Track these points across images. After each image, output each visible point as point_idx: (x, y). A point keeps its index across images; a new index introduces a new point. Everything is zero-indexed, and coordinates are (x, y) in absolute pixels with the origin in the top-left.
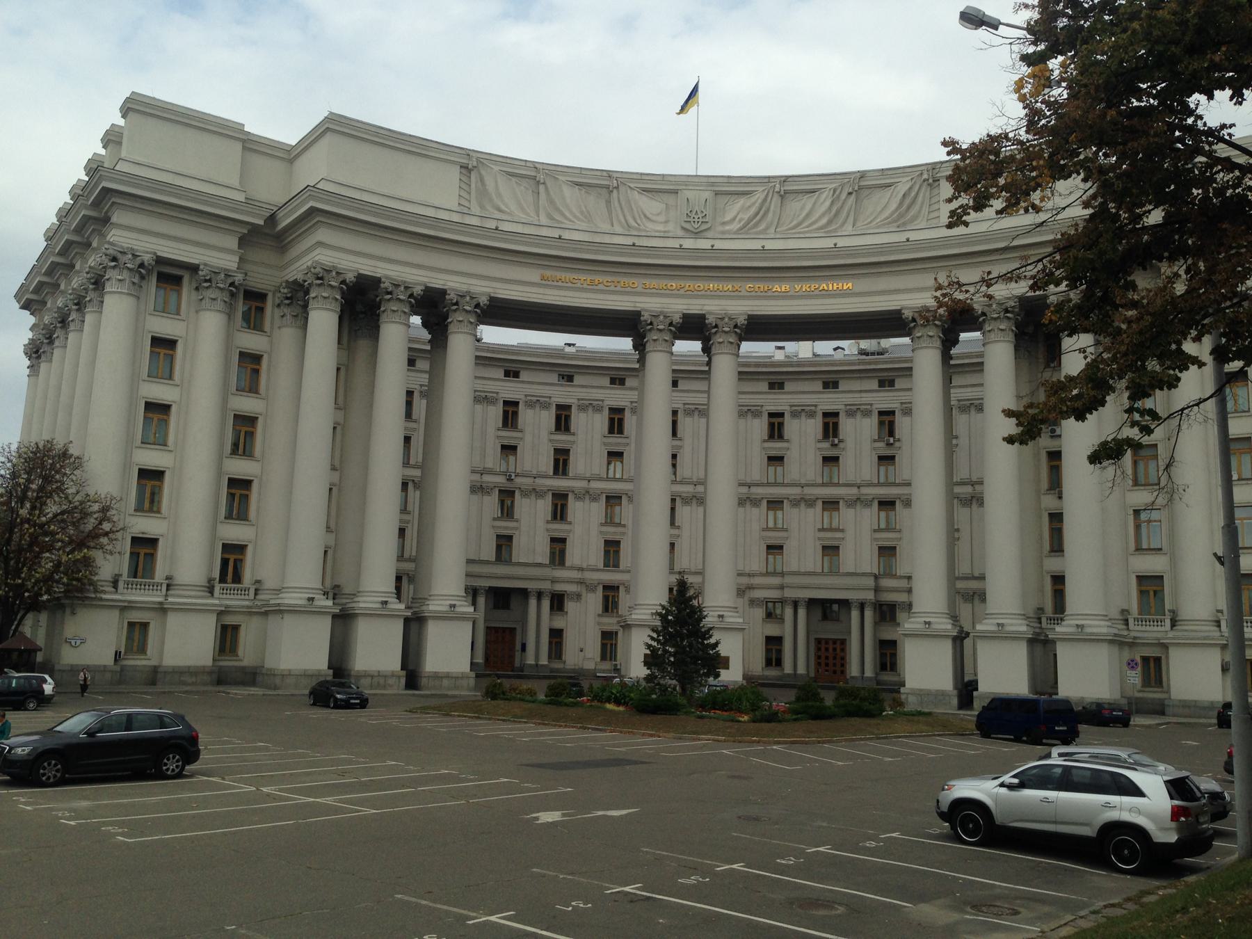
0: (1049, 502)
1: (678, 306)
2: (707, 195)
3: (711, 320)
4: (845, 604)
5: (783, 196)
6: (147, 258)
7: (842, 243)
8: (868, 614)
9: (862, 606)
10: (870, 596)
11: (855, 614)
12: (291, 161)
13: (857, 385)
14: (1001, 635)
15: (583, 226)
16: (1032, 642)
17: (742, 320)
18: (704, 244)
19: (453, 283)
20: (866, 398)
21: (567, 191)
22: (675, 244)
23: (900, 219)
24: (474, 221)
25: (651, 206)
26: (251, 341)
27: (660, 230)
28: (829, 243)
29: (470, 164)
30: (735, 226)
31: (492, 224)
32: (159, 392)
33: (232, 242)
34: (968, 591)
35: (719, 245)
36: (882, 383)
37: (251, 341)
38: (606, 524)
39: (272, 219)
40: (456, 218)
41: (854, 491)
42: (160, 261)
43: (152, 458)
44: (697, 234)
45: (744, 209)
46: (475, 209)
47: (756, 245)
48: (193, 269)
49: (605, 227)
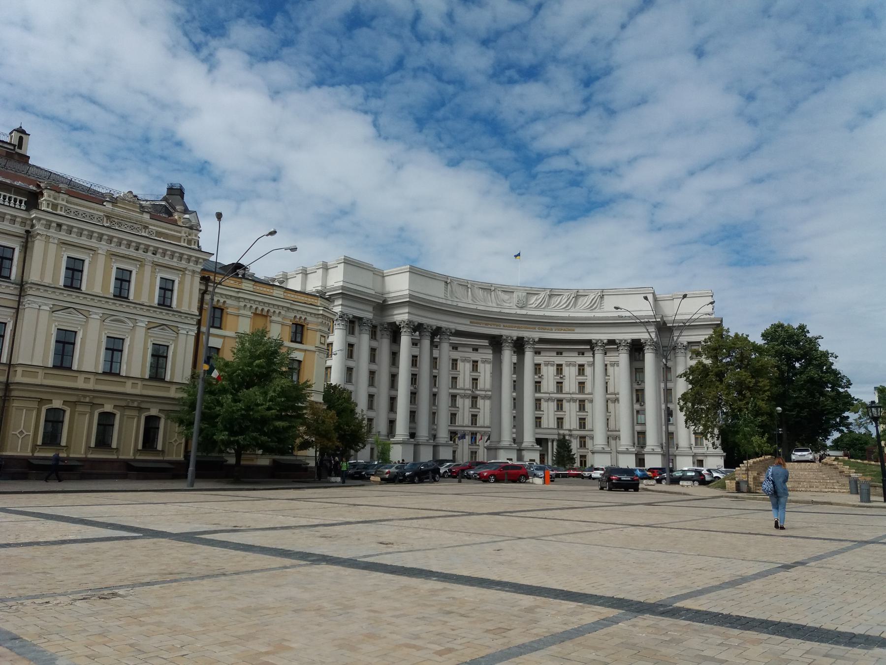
0: (637, 407)
1: (515, 334)
2: (524, 294)
3: (526, 339)
4: (547, 440)
5: (550, 296)
6: (351, 316)
7: (572, 315)
8: (555, 444)
9: (553, 441)
10: (556, 437)
11: (550, 444)
12: (383, 277)
13: (548, 354)
14: (627, 452)
15: (483, 304)
16: (636, 454)
17: (537, 340)
18: (523, 312)
19: (443, 325)
20: (552, 359)
21: (481, 291)
22: (513, 311)
23: (591, 308)
24: (449, 302)
25: (506, 297)
26: (375, 344)
27: (510, 306)
28: (566, 314)
29: (447, 282)
30: (534, 306)
31: (455, 304)
32: (351, 364)
33: (371, 309)
34: (612, 436)
35: (530, 313)
36: (557, 353)
37: (352, 340)
38: (452, 406)
39: (385, 301)
40: (444, 301)
41: (547, 395)
42: (354, 317)
43: (350, 387)
44: (522, 308)
45: (536, 300)
46: (449, 298)
47: (541, 313)
48: (360, 319)
49: (490, 304)
